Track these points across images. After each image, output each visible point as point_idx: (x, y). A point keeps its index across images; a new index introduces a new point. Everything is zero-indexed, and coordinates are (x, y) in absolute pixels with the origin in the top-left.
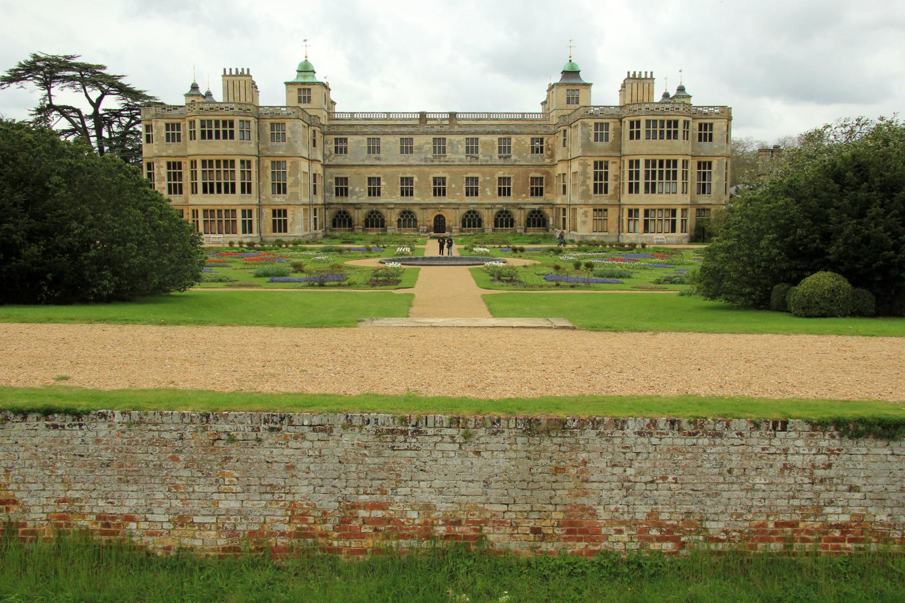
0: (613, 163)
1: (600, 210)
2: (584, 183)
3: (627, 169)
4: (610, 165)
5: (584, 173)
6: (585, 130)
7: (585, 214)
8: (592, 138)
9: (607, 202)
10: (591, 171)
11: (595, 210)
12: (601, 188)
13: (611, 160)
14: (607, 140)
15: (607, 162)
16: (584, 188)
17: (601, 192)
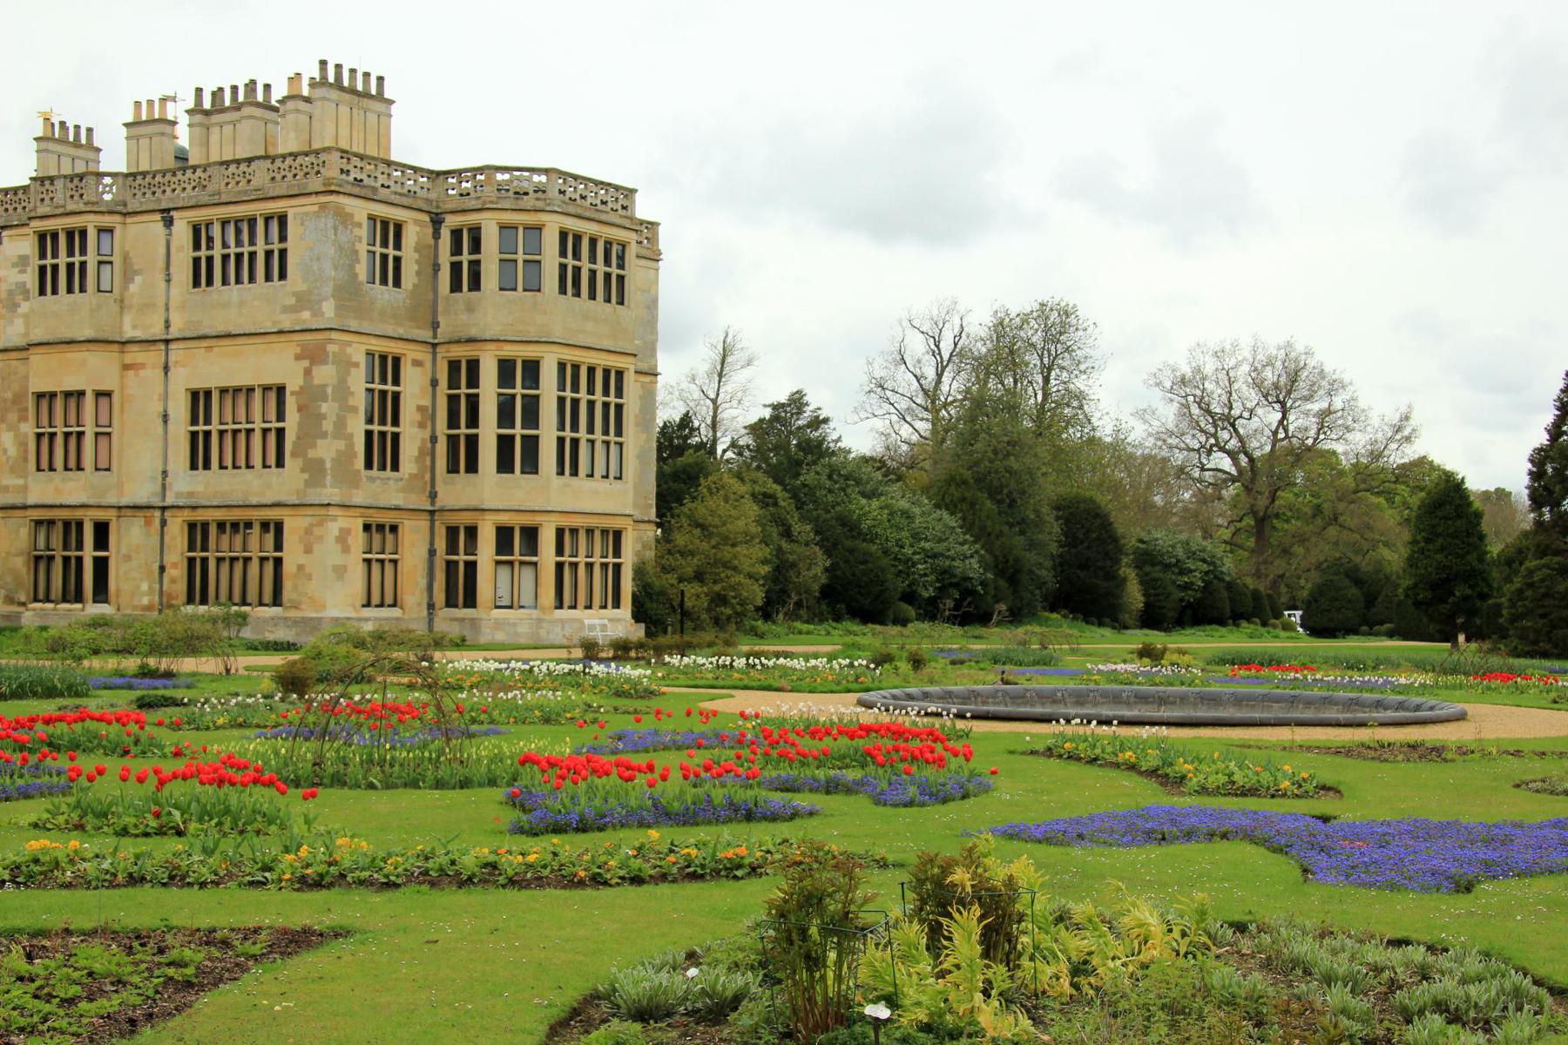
0: (417, 363)
1: (381, 528)
2: (341, 423)
3: (489, 391)
4: (407, 370)
5: (343, 392)
6: (343, 238)
7: (343, 538)
8: (362, 270)
9: (398, 500)
10: (358, 383)
11: (367, 527)
12: (382, 451)
13: (410, 353)
14: (397, 283)
15: (397, 361)
16: (341, 445)
17: (383, 467)
